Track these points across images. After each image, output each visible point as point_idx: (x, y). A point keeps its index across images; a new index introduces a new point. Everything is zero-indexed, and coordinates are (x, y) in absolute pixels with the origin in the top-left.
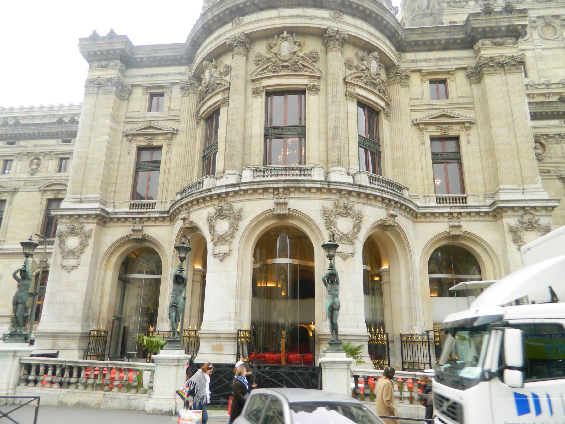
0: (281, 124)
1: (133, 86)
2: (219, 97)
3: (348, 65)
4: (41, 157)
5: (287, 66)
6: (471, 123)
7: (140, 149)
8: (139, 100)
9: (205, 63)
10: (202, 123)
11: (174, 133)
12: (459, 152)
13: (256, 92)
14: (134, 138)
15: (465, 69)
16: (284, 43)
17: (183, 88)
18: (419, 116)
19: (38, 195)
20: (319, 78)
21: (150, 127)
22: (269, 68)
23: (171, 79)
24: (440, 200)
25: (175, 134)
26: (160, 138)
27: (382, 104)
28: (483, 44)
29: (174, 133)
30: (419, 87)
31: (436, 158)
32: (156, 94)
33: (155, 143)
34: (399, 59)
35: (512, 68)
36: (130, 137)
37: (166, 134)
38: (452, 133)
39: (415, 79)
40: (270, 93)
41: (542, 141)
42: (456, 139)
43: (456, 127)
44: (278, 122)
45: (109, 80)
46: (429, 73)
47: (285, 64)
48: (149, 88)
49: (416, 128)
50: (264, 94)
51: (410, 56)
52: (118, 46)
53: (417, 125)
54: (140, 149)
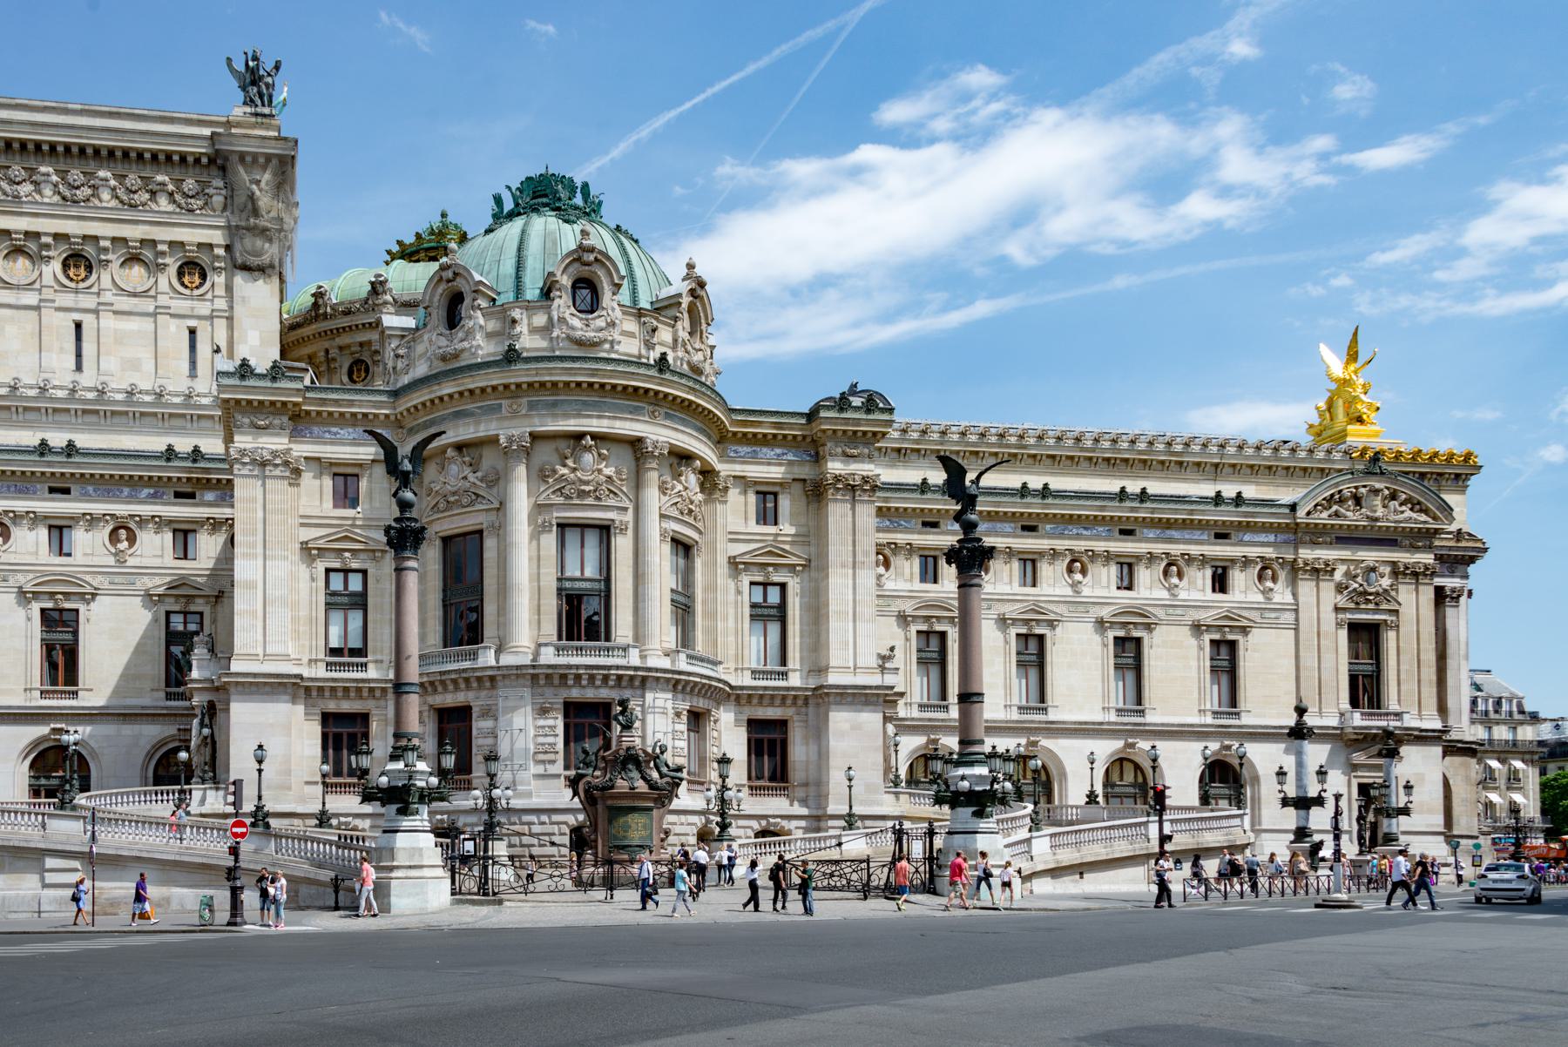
0: (578, 574)
3: (663, 490)
9: (450, 452)
10: (438, 542)
21: (346, 538)
22: (566, 491)
31: (760, 614)
40: (562, 527)
44: (572, 571)
54: (328, 571)
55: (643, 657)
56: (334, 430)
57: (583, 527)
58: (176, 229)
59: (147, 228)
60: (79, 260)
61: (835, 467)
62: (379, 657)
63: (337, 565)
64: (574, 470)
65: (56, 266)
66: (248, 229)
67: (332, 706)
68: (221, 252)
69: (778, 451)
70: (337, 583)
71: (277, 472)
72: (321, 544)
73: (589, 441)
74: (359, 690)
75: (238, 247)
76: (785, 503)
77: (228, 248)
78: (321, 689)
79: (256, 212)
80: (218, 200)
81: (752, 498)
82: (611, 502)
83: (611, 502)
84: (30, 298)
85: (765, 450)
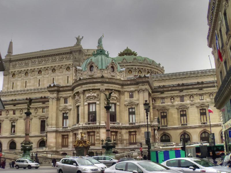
1: (60, 97)
2: (78, 104)
7: (63, 114)
8: (62, 100)
9: (75, 94)
11: (71, 110)
17: (72, 98)
18: (126, 103)
19: (38, 119)
23: (69, 95)
24: (130, 124)
27: (116, 102)
28: (140, 85)
29: (71, 110)
30: (127, 95)
34: (122, 88)
44: (91, 110)
45: (55, 97)
51: (125, 87)
52: (56, 88)
53: (125, 105)
54: (63, 114)
55: (100, 124)
57: (93, 103)
59: (62, 63)
60: (54, 70)
63: (64, 112)
66: (75, 61)
67: (63, 134)
68: (72, 65)
70: (65, 115)
73: (91, 90)
74: (66, 131)
75: (74, 64)
77: (73, 64)
79: (76, 58)
80: (72, 58)
84: (47, 76)
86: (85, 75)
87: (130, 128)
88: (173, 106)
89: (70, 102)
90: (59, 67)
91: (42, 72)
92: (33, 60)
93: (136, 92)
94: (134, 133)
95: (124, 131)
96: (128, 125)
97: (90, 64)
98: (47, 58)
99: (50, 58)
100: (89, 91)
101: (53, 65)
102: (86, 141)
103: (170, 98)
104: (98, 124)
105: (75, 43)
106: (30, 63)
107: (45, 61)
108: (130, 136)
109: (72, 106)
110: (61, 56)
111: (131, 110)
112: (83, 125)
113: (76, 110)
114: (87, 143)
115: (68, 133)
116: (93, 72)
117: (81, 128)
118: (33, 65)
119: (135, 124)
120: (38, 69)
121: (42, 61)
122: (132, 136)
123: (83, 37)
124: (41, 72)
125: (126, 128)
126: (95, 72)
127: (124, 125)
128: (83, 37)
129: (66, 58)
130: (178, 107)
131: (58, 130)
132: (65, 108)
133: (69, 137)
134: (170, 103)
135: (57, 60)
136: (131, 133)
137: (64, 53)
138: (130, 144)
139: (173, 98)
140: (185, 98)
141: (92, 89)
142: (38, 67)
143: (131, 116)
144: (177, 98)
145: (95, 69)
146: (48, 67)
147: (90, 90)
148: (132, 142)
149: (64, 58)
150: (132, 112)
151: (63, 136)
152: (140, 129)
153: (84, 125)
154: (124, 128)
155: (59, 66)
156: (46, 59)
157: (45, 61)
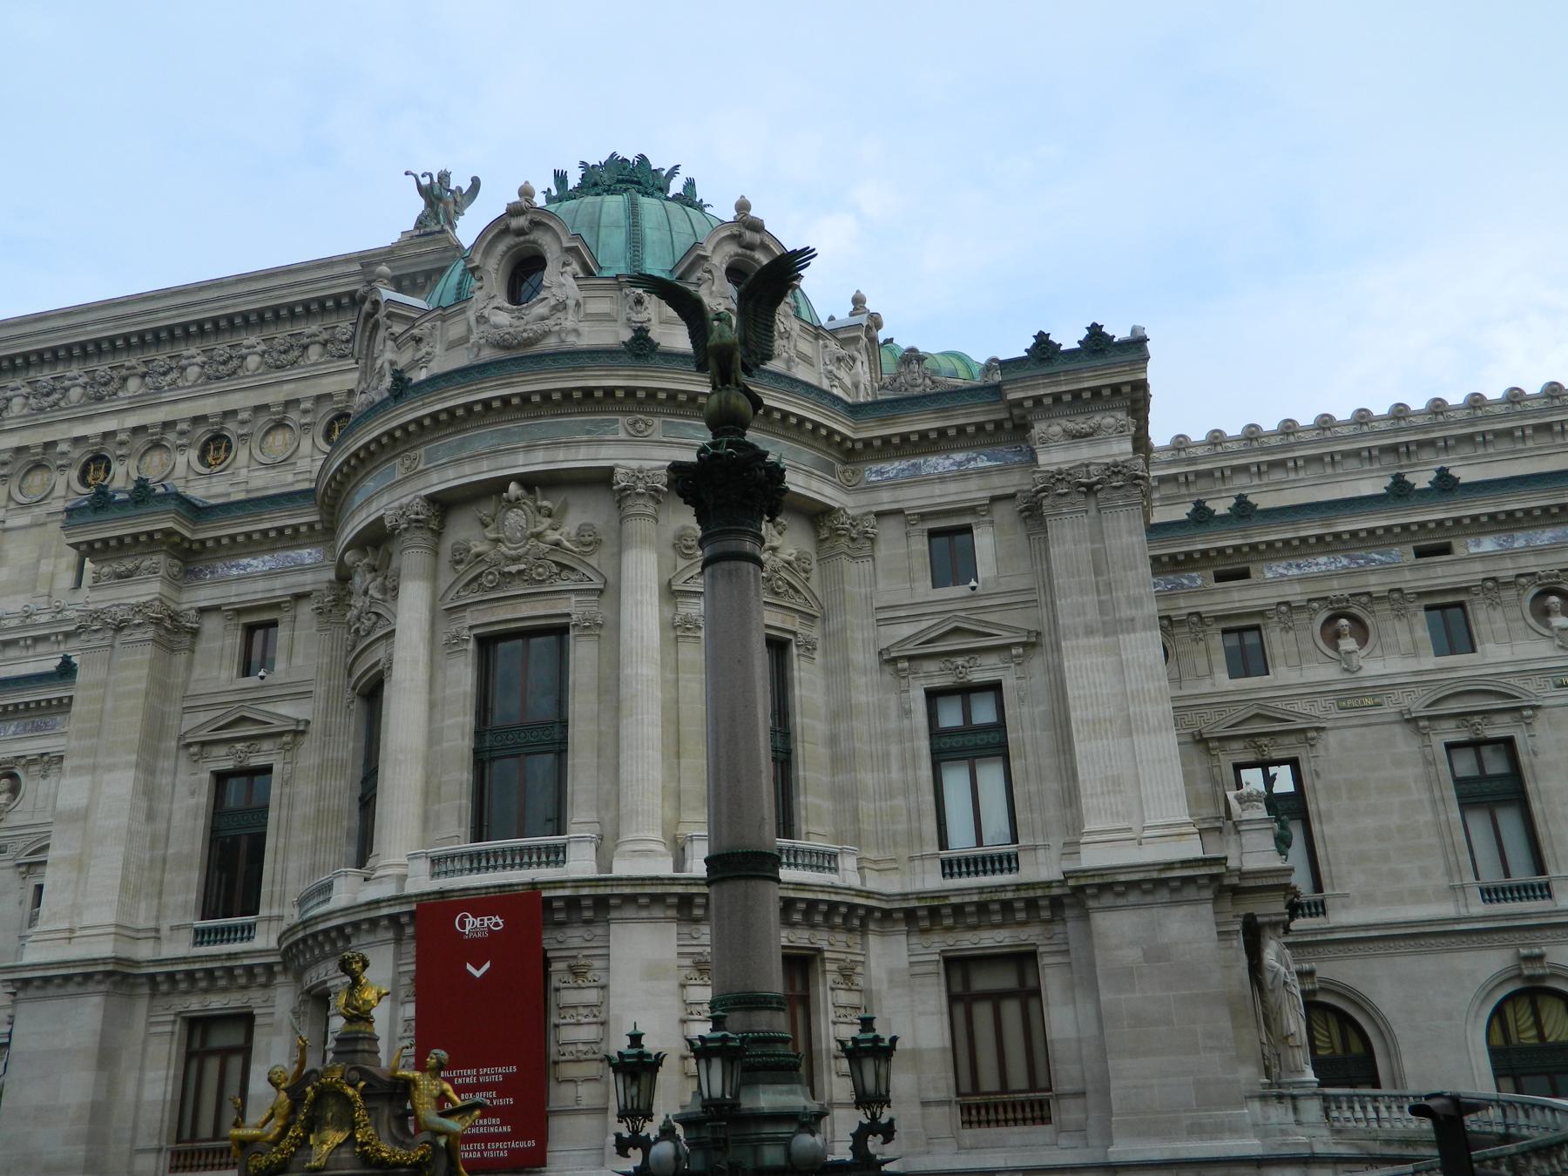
1: (202, 611)
4: (18, 771)
5: (520, 572)
6: (1024, 645)
7: (221, 778)
12: (1000, 726)
13: (456, 642)
14: (207, 749)
15: (1012, 497)
16: (511, 514)
17: (320, 612)
20: (601, 591)
21: (243, 720)
24: (950, 867)
25: (303, 732)
26: (266, 745)
29: (299, 732)
31: (950, 748)
32: (257, 630)
33: (256, 761)
34: (848, 488)
35: (1115, 494)
36: (194, 749)
37: (281, 734)
38: (977, 677)
39: (889, 532)
40: (487, 643)
41: (1355, 610)
42: (995, 687)
43: (992, 660)
45: (138, 609)
46: (923, 517)
47: (514, 568)
48: (239, 612)
49: (888, 669)
50: (471, 646)
51: (872, 472)
53: (889, 660)
54: (221, 778)
55: (604, 860)
56: (244, 561)
58: (325, 381)
61: (1053, 458)
62: (275, 912)
63: (228, 765)
64: (497, 541)
65: (193, 454)
67: (195, 1004)
69: (959, 457)
71: (138, 635)
72: (204, 735)
74: (229, 971)
76: (984, 541)
78: (171, 976)
81: (921, 545)
82: (560, 585)
83: (560, 585)
85: (933, 460)
86: (452, 346)
87: (958, 910)
88: (1357, 699)
89: (302, 652)
90: (263, 420)
91: (115, 466)
92: (45, 376)
93: (1004, 512)
94: (1003, 979)
95: (887, 957)
96: (931, 880)
97: (506, 231)
98: (168, 350)
99: (192, 351)
100: (487, 509)
101: (210, 406)
102: (403, 1089)
103: (1323, 615)
104: (581, 864)
105: (410, 225)
106: (18, 402)
107: (143, 376)
108: (960, 1011)
109: (320, 690)
110: (282, 334)
111: (950, 717)
112: (403, 878)
113: (349, 726)
114: (428, 1112)
115: (253, 999)
116: (540, 310)
117: (374, 923)
118: (41, 410)
119: (1007, 862)
120: (77, 441)
121: (125, 379)
122: (983, 1013)
123: (476, 183)
124: (108, 470)
125: (919, 916)
126: (561, 307)
127: (891, 884)
128: (476, 183)
129: (324, 344)
130: (1418, 708)
131: (137, 964)
132: (239, 724)
133: (260, 1039)
134: (1325, 672)
135: (253, 361)
136: (966, 982)
137: (314, 307)
138: (966, 1109)
139: (1353, 619)
140: (1483, 618)
141: (530, 482)
142: (79, 430)
143: (956, 781)
144: (1399, 617)
145: (559, 280)
146: (168, 425)
147: (500, 485)
148: (989, 1081)
149: (305, 347)
150: (968, 729)
151: (197, 1025)
152: (1085, 916)
153: (422, 882)
154: (887, 915)
155: (266, 407)
156: (161, 357)
157: (143, 376)
